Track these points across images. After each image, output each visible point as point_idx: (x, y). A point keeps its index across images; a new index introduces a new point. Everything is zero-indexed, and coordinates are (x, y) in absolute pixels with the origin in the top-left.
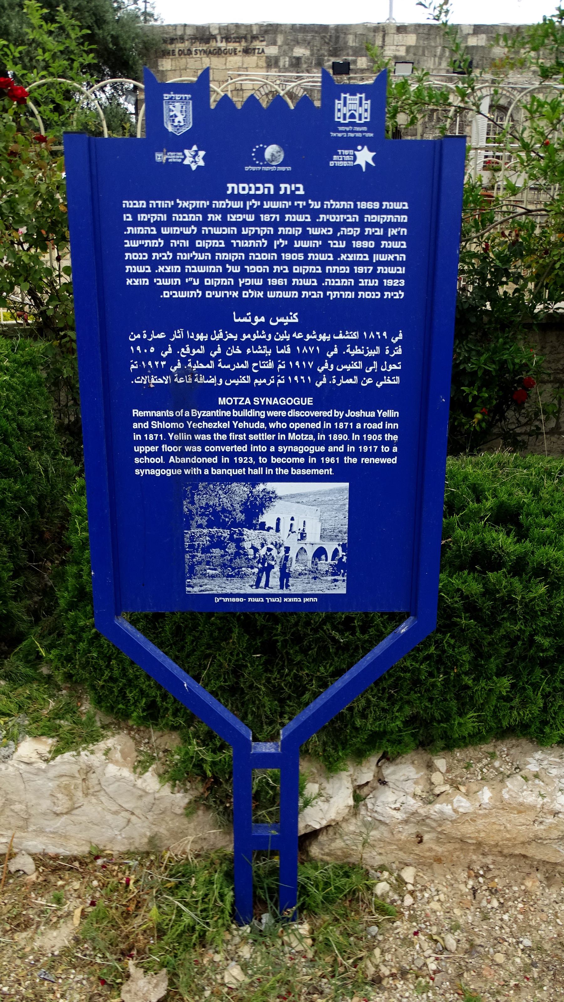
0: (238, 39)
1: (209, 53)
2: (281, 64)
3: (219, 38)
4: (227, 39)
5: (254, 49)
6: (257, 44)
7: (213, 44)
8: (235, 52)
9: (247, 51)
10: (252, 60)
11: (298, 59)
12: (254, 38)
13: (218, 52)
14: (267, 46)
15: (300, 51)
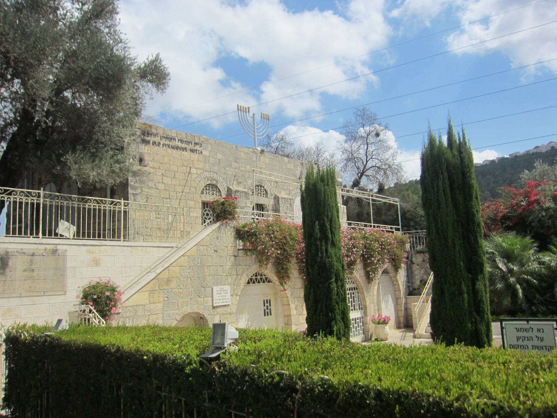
0: (188, 143)
1: (173, 148)
2: (211, 162)
3: (177, 140)
4: (182, 141)
5: (196, 150)
6: (197, 147)
7: (173, 143)
8: (185, 149)
9: (192, 151)
10: (195, 156)
11: (219, 160)
12: (196, 144)
13: (177, 148)
14: (203, 149)
15: (219, 156)
